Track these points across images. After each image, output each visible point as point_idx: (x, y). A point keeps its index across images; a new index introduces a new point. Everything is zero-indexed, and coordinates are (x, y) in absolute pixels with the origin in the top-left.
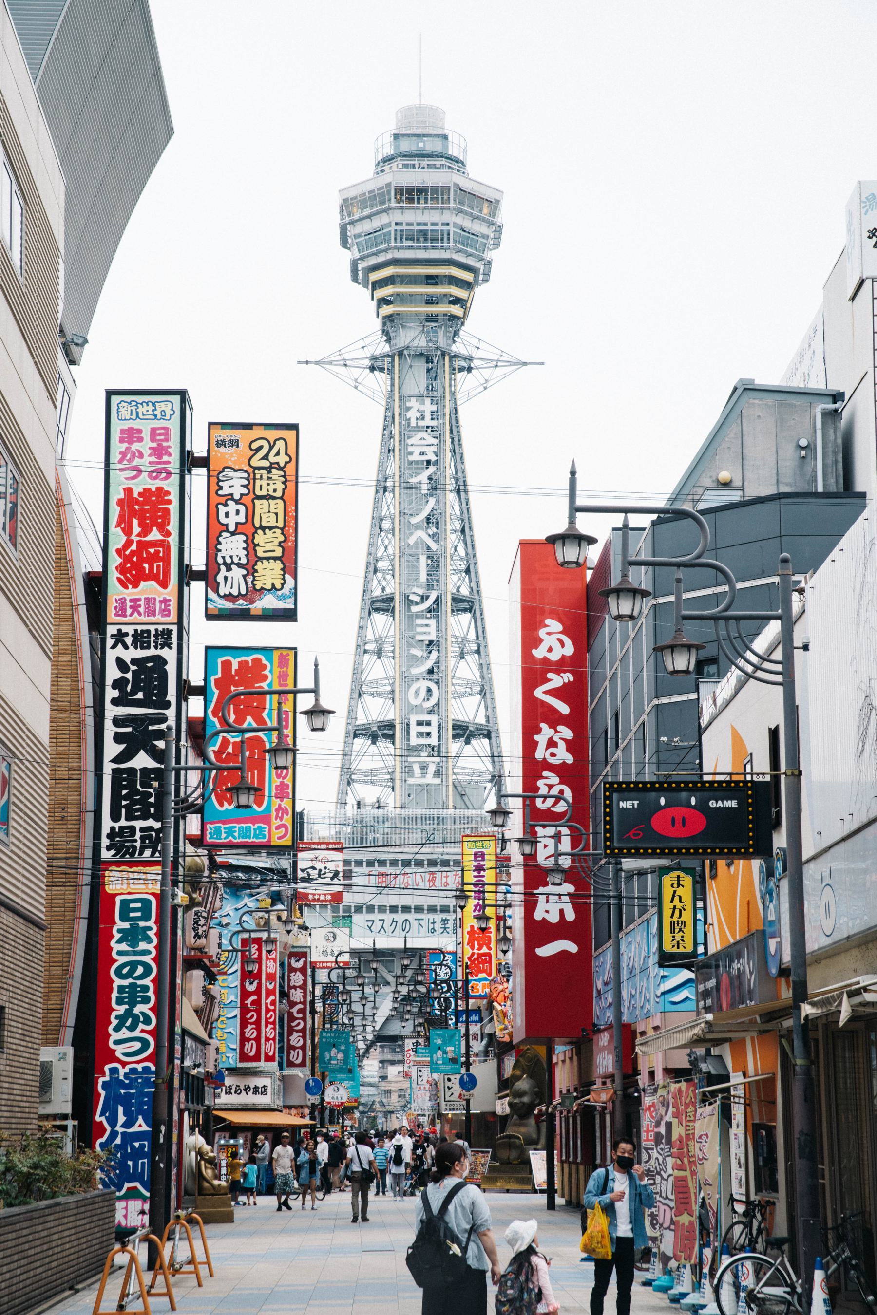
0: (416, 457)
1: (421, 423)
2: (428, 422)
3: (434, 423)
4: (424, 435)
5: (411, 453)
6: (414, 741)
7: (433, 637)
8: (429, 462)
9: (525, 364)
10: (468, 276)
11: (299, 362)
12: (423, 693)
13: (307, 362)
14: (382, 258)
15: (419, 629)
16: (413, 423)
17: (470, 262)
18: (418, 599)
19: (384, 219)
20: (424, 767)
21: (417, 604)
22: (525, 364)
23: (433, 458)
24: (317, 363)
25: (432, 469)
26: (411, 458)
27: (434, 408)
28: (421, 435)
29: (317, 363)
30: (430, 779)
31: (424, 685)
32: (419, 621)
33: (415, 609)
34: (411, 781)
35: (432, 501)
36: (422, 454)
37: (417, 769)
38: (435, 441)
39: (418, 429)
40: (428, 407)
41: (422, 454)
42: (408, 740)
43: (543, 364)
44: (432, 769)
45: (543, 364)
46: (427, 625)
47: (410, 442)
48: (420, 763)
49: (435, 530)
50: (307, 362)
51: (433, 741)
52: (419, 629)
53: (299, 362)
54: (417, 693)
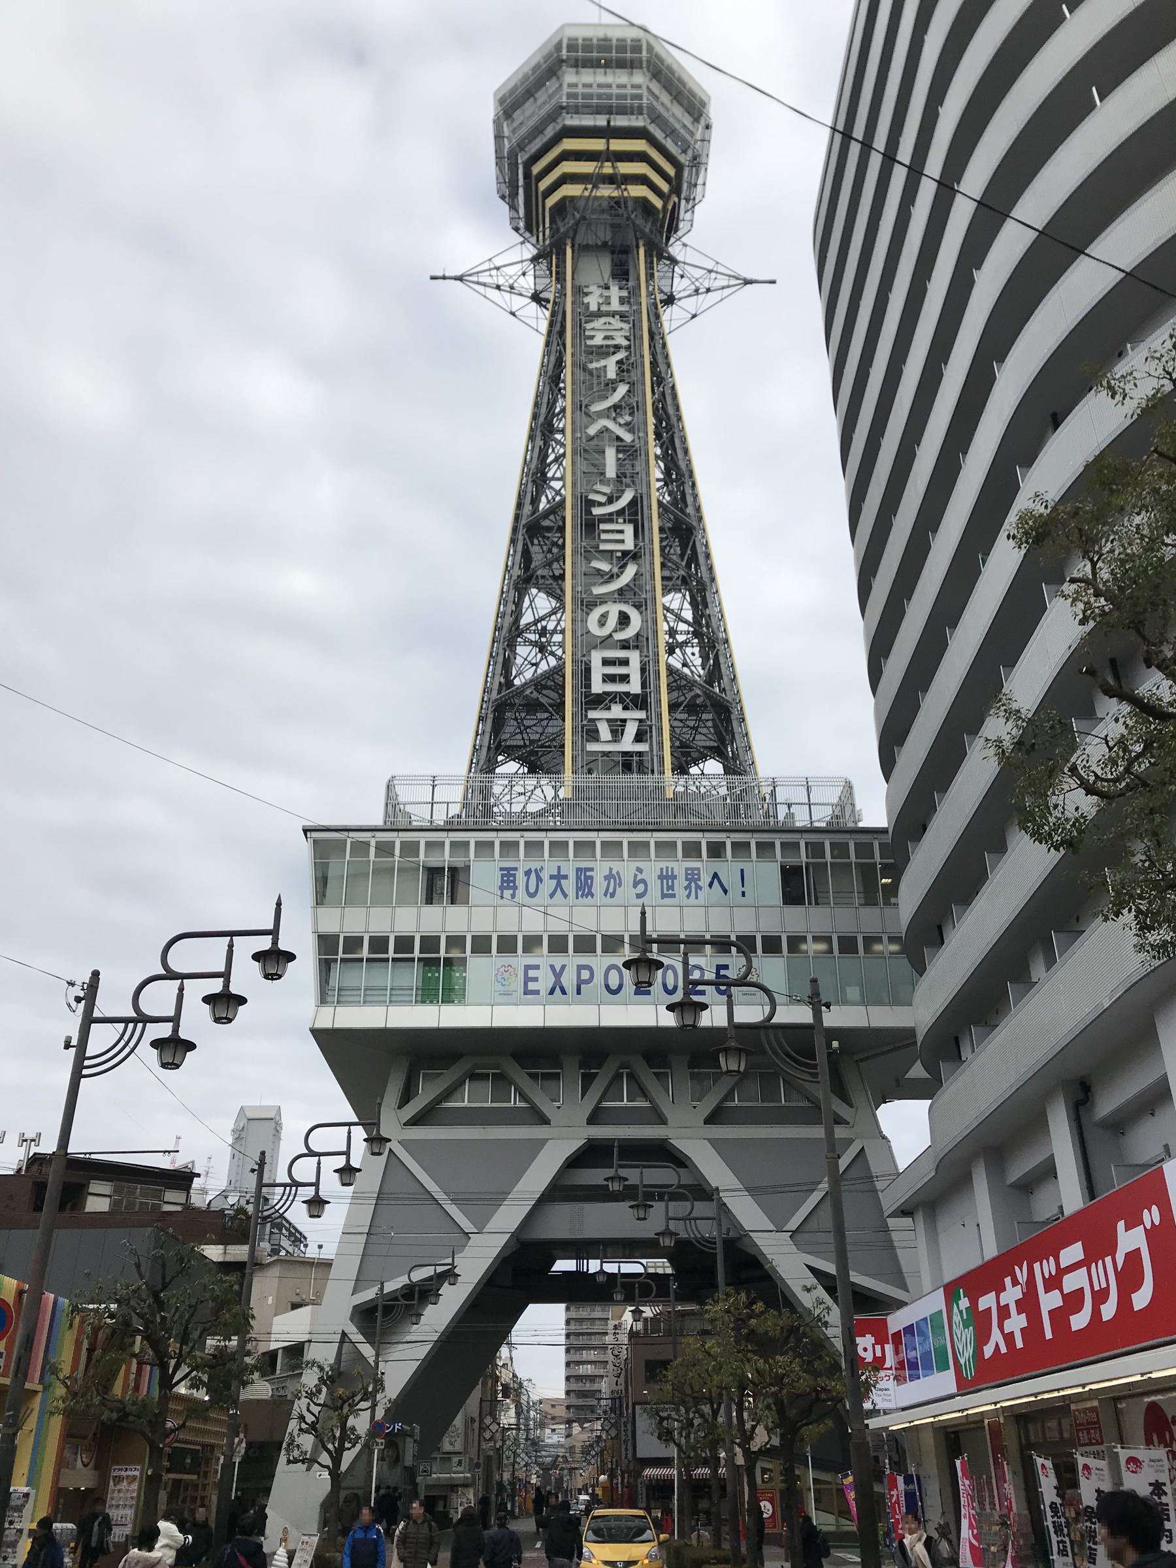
0: (598, 340)
1: (604, 308)
2: (615, 305)
3: (625, 308)
4: (611, 320)
5: (592, 337)
6: (598, 687)
7: (629, 545)
8: (617, 348)
9: (747, 282)
10: (671, 171)
11: (433, 278)
12: (612, 621)
13: (444, 278)
14: (550, 132)
15: (604, 536)
16: (593, 307)
17: (669, 145)
18: (603, 499)
19: (551, 85)
20: (618, 728)
21: (600, 504)
22: (747, 282)
23: (625, 343)
24: (460, 279)
25: (621, 355)
26: (589, 342)
27: (625, 293)
28: (603, 320)
29: (460, 279)
30: (627, 744)
31: (614, 610)
32: (603, 527)
33: (597, 511)
34: (592, 747)
35: (622, 389)
36: (606, 338)
37: (605, 732)
38: (626, 326)
39: (599, 314)
40: (615, 293)
41: (606, 338)
42: (588, 686)
43: (774, 282)
44: (631, 730)
45: (774, 282)
46: (621, 532)
47: (589, 326)
48: (608, 720)
49: (628, 418)
50: (444, 278)
51: (635, 687)
52: (604, 536)
53: (433, 278)
54: (602, 622)
